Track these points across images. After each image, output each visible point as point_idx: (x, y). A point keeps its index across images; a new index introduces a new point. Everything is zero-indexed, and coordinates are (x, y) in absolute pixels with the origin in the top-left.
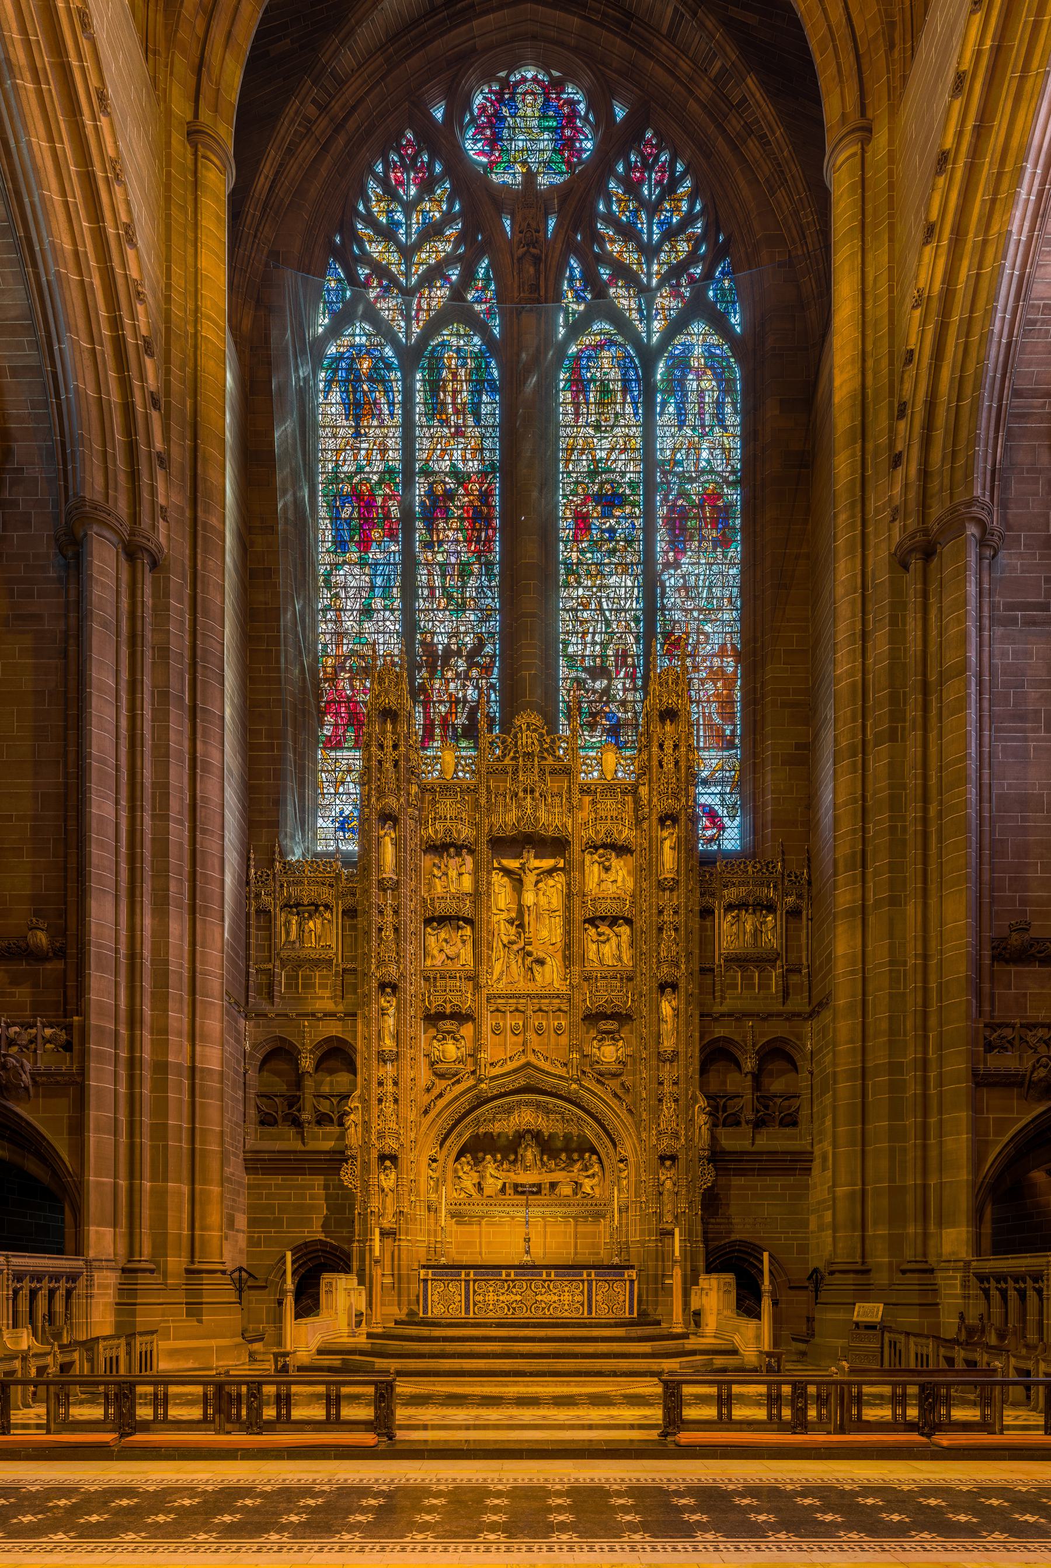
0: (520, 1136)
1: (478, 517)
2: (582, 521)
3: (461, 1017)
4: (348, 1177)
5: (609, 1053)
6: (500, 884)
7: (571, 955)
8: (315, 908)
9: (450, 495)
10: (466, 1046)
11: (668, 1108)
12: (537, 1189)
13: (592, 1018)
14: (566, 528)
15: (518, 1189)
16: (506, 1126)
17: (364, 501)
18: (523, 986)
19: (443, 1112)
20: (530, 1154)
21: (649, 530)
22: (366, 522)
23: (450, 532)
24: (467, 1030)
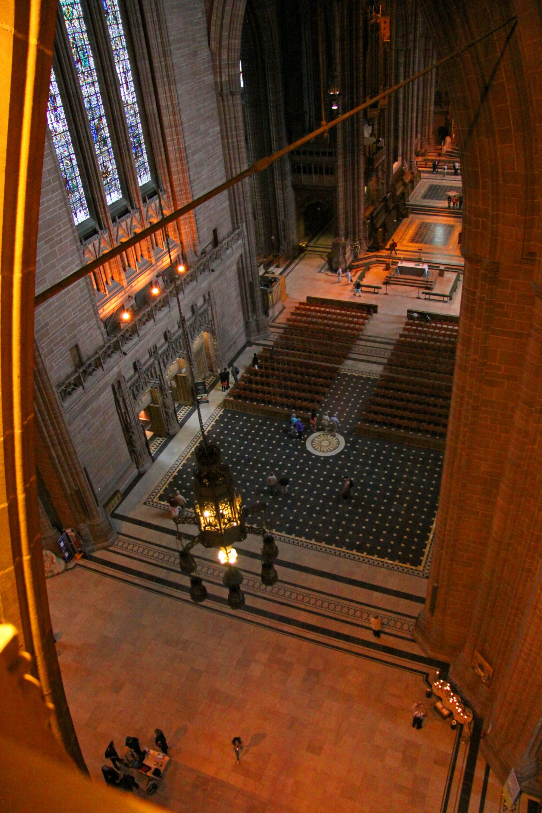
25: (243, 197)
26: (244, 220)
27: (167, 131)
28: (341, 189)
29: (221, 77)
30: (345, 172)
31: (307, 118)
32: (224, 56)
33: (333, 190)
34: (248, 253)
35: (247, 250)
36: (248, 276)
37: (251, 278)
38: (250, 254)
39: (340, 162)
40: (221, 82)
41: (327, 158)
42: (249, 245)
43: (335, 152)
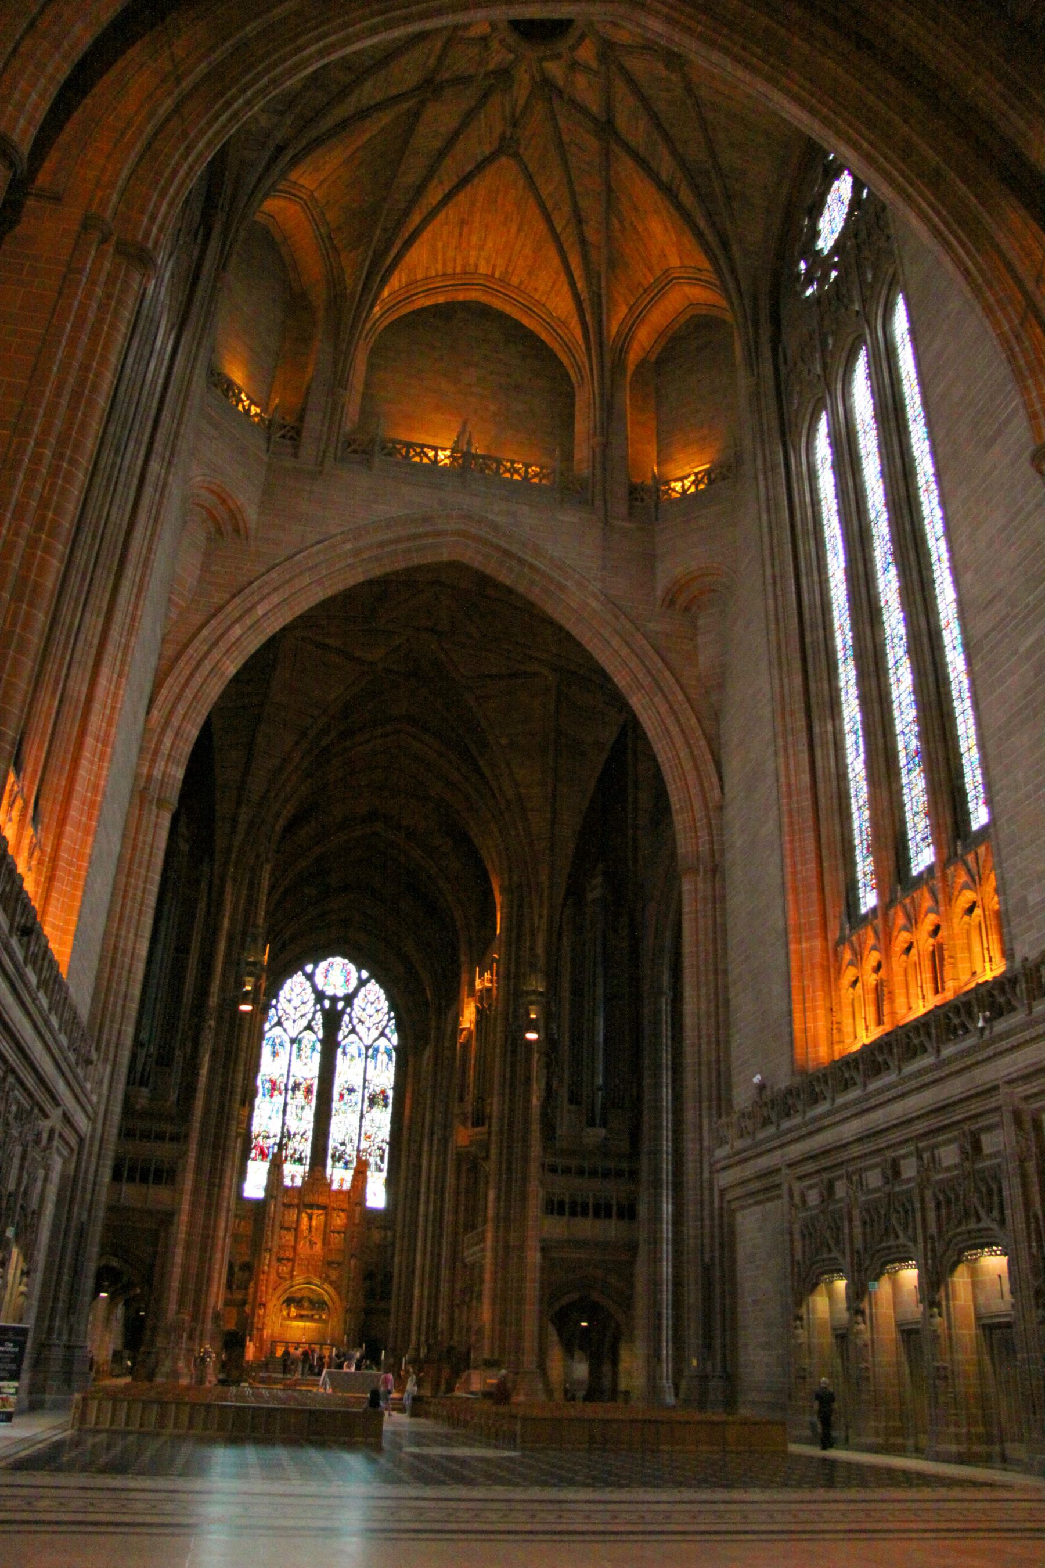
1: (308, 1091)
2: (342, 1096)
3: (288, 1260)
4: (247, 1308)
5: (334, 1275)
6: (304, 1217)
7: (325, 1242)
11: (351, 1294)
13: (330, 1264)
14: (336, 1096)
16: (298, 1295)
17: (273, 1083)
18: (309, 1251)
20: (306, 1304)
22: (273, 1089)
23: (300, 1094)
24: (290, 1264)
26: (111, 1057)
27: (89, 740)
28: (184, 1218)
29: (151, 767)
32: (167, 742)
33: (167, 1218)
34: (97, 1143)
38: (100, 1148)
40: (150, 776)
41: (168, 1145)
42: (104, 1124)
43: (186, 1136)
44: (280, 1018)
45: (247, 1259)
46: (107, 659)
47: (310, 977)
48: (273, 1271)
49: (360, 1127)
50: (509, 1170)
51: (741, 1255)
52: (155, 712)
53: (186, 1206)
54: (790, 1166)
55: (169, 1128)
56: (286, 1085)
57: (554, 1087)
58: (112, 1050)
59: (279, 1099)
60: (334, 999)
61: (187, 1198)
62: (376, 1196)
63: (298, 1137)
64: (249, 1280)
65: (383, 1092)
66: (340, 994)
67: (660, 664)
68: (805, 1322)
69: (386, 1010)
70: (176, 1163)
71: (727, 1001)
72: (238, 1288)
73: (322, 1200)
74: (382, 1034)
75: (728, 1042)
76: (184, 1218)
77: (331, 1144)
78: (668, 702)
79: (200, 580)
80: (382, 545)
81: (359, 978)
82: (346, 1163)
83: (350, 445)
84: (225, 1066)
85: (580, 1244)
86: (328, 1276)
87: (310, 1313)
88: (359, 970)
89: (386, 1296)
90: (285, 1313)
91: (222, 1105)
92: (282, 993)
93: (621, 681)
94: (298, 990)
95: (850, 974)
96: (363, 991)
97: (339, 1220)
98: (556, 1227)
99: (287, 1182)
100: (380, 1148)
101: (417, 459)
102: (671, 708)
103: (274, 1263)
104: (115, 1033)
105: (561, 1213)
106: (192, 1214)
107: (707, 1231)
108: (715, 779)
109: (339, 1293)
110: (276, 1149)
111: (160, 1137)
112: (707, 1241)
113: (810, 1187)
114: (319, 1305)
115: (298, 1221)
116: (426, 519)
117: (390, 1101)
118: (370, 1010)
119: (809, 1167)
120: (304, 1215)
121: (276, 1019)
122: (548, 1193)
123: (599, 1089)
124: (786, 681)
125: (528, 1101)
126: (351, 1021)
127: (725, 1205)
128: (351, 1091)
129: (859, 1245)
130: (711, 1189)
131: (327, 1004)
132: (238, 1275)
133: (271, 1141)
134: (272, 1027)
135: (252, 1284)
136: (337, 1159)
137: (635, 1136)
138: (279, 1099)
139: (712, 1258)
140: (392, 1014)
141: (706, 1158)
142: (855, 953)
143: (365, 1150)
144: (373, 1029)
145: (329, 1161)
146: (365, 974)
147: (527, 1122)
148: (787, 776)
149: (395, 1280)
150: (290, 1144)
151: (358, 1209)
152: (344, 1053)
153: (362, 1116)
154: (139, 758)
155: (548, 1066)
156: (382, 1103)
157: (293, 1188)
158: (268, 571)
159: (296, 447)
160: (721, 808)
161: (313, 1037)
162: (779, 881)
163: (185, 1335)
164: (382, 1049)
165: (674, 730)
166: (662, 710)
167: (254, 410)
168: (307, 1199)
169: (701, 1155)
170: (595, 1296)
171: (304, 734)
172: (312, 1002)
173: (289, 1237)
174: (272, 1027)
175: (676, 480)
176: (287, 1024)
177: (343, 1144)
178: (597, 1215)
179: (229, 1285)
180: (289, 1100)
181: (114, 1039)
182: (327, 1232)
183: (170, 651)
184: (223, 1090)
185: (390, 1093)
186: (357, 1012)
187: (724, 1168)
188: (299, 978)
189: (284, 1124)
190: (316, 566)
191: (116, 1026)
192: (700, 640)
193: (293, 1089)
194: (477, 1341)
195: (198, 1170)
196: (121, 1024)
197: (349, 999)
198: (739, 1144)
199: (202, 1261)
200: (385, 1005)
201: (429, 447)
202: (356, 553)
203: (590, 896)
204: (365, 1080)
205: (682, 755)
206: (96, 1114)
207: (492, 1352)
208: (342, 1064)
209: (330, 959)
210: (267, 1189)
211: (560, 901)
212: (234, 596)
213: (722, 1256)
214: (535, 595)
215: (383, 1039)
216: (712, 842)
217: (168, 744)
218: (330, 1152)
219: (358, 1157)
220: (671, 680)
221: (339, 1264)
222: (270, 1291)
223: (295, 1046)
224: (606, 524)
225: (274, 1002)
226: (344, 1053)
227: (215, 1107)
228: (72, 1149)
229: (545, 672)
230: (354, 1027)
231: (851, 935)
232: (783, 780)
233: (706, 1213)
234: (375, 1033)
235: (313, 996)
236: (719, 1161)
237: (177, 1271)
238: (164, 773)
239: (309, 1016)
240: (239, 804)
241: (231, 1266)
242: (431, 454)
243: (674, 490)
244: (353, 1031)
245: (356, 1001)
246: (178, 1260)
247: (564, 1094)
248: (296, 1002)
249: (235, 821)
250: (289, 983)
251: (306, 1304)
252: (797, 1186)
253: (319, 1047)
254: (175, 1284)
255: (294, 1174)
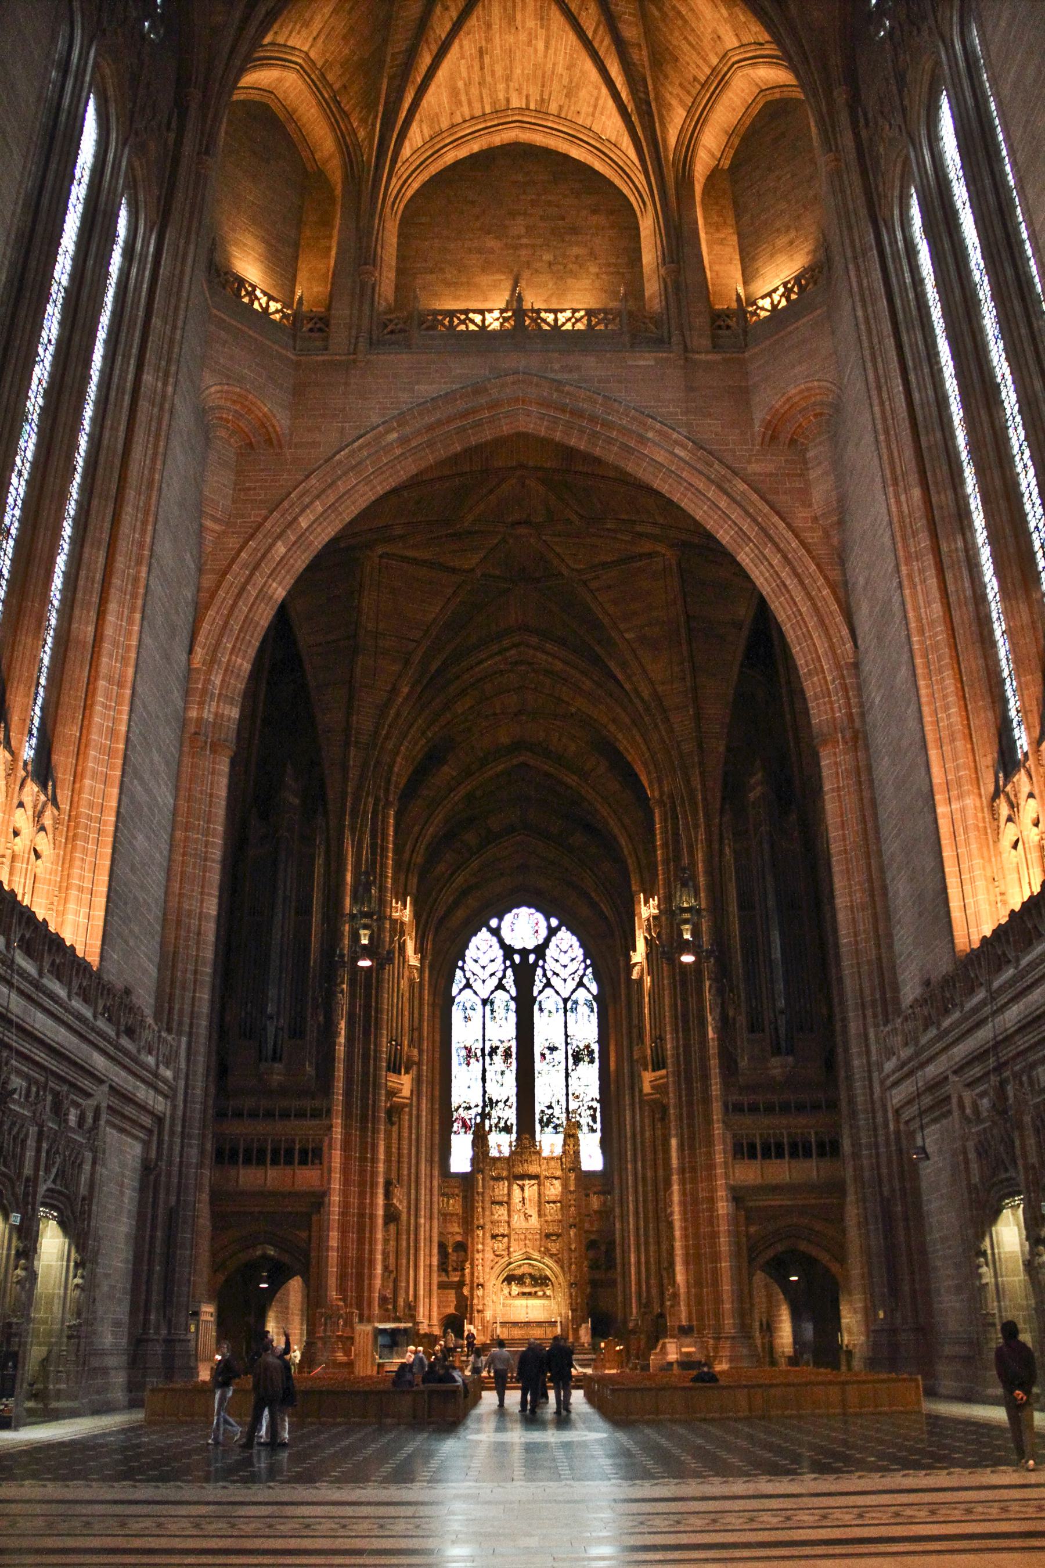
0: (524, 1275)
1: (507, 1054)
2: (543, 1055)
3: (503, 1236)
4: (466, 1291)
5: (554, 1247)
8: (453, 1196)
9: (497, 1048)
10: (505, 1245)
12: (530, 1294)
13: (548, 1236)
14: (537, 1057)
15: (524, 1294)
17: (468, 1050)
18: (524, 1224)
19: (497, 1269)
20: (528, 1281)
21: (567, 1058)
25: (196, 972)
26: (186, 1029)
27: (102, 683)
28: (335, 1198)
30: (346, 1159)
31: (271, 1030)
33: (318, 1200)
35: (180, 1113)
36: (167, 1194)
37: (173, 1199)
38: (183, 1127)
39: (338, 1132)
42: (185, 1101)
43: (329, 1111)
44: (468, 980)
45: (459, 1238)
46: (114, 595)
47: (496, 932)
48: (487, 1248)
49: (567, 1086)
50: (691, 1116)
51: (924, 1185)
52: (199, 651)
53: (336, 1185)
54: (955, 1072)
55: (308, 1104)
56: (483, 1050)
57: (731, 1014)
58: (186, 1020)
59: (476, 1067)
60: (524, 953)
61: (336, 1176)
62: (592, 1158)
63: (501, 1105)
64: (464, 1261)
65: (588, 1047)
66: (530, 947)
67: (766, 509)
68: (990, 1257)
69: (581, 958)
70: (321, 1141)
71: (884, 888)
72: (455, 1270)
73: (533, 1169)
74: (581, 984)
75: (890, 936)
76: (335, 1198)
77: (538, 1109)
78: (779, 550)
79: (234, 502)
80: (430, 428)
81: (549, 927)
82: (555, 1127)
83: (386, 326)
84: (367, 1032)
85: (776, 1189)
86: (547, 1250)
87: (533, 1290)
88: (547, 920)
89: (611, 1265)
90: (506, 1291)
91: (366, 1073)
92: (467, 952)
93: (725, 536)
94: (484, 947)
95: (1009, 833)
96: (554, 939)
97: (554, 1190)
98: (749, 1173)
99: (494, 1153)
100: (590, 1108)
101: (463, 327)
102: (785, 557)
103: (488, 1240)
104: (188, 1001)
105: (753, 1156)
106: (345, 1194)
107: (883, 1159)
108: (845, 632)
109: (562, 1267)
110: (478, 1120)
111: (301, 1115)
112: (884, 1171)
113: (982, 1095)
114: (541, 1281)
115: (509, 1194)
116: (478, 390)
117: (596, 1055)
118: (564, 959)
119: (977, 1071)
120: (515, 1187)
121: (464, 981)
122: (734, 1136)
123: (782, 1012)
124: (903, 498)
125: (705, 1034)
126: (545, 975)
127: (902, 1127)
128: (553, 1049)
129: (1033, 1159)
130: (885, 1111)
131: (517, 958)
132: (453, 1257)
133: (473, 1112)
134: (461, 990)
135: (468, 1265)
136: (545, 1124)
137: (830, 1064)
138: (476, 1067)
139: (893, 1191)
140: (588, 962)
141: (875, 1074)
142: (1012, 805)
143: (574, 1112)
144: (569, 980)
145: (538, 1127)
146: (554, 922)
147: (704, 1059)
148: (917, 609)
149: (618, 1250)
150: (494, 1114)
151: (572, 1176)
152: (541, 1010)
153: (567, 1075)
154: (186, 702)
155: (720, 992)
156: (586, 1059)
157: (499, 1159)
158: (307, 477)
159: (326, 339)
160: (856, 665)
161: (507, 997)
162: (919, 736)
163: (341, 1322)
164: (581, 1002)
165: (791, 582)
166: (775, 562)
167: (274, 306)
168: (519, 1170)
169: (870, 1071)
170: (803, 1246)
171: (407, 663)
172: (501, 959)
173: (501, 1212)
174: (461, 990)
175: (763, 298)
176: (477, 985)
177: (550, 1107)
178: (794, 1155)
179: (443, 1267)
180: (487, 1066)
181: (187, 1008)
182: (541, 1202)
183: (208, 580)
184: (366, 1057)
185: (595, 1047)
186: (550, 964)
187: (896, 1084)
188: (484, 933)
189: (485, 1092)
190: (359, 463)
191: (189, 995)
192: (812, 475)
193: (490, 1055)
194: (672, 1306)
195: (346, 1146)
196: (194, 991)
197: (540, 951)
198: (905, 1053)
199: (361, 1241)
200: (579, 953)
201: (475, 311)
202: (403, 441)
203: (752, 796)
204: (567, 1036)
205: (804, 610)
206: (174, 1089)
207: (690, 1320)
208: (539, 1020)
209: (515, 911)
210: (474, 1161)
211: (718, 806)
212: (271, 512)
213: (903, 1189)
214: (611, 455)
215: (581, 990)
216: (848, 705)
217: (218, 682)
218: (537, 1117)
219: (568, 1119)
220: (782, 525)
221: (558, 1235)
222: (487, 1270)
223: (488, 1008)
224: (686, 359)
225: (460, 963)
226: (541, 1010)
227: (357, 1077)
228: (150, 1132)
229: (660, 548)
230: (548, 980)
231: (1005, 785)
232: (911, 615)
233: (881, 1139)
234: (572, 984)
235: (501, 952)
236: (888, 1076)
237: (333, 1255)
238: (216, 714)
239: (500, 974)
240: (347, 744)
241: (442, 1246)
242: (478, 318)
243: (763, 309)
244: (548, 984)
245: (548, 952)
246: (334, 1243)
247: (742, 1020)
248: (483, 961)
249: (345, 769)
250: (475, 941)
251: (528, 1281)
252: (968, 1096)
253: (513, 1005)
254: (333, 1269)
255: (500, 1144)
